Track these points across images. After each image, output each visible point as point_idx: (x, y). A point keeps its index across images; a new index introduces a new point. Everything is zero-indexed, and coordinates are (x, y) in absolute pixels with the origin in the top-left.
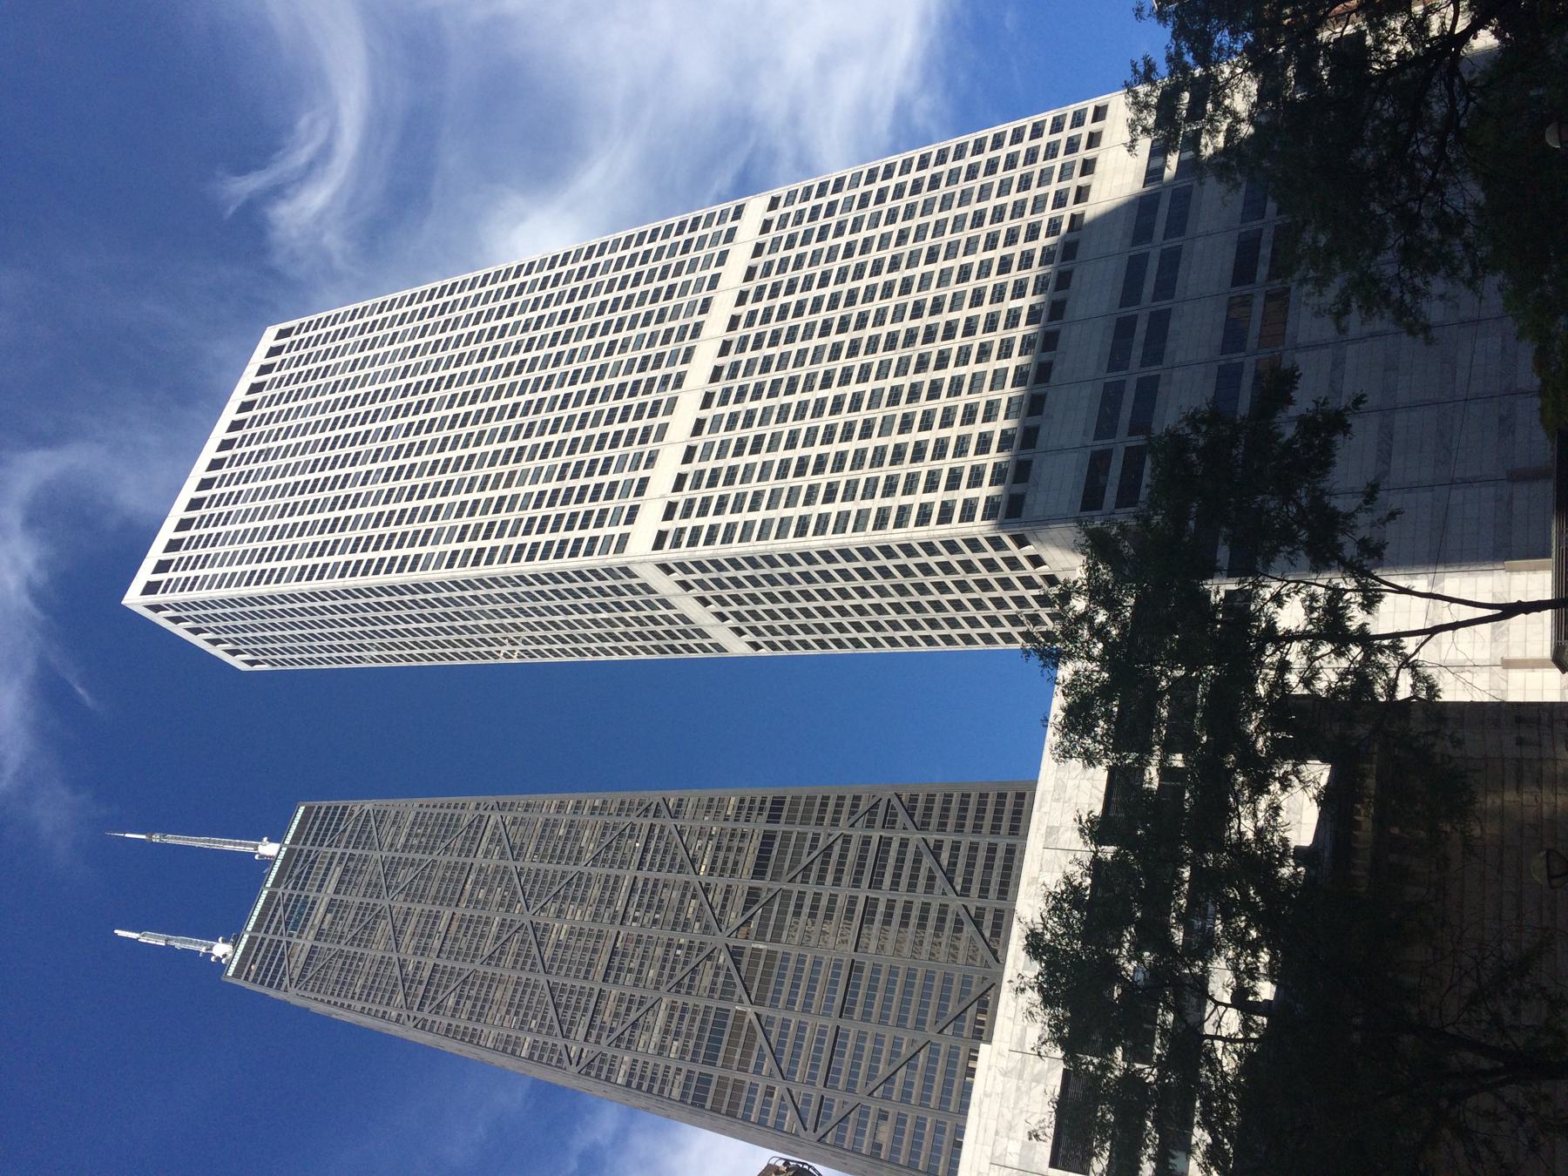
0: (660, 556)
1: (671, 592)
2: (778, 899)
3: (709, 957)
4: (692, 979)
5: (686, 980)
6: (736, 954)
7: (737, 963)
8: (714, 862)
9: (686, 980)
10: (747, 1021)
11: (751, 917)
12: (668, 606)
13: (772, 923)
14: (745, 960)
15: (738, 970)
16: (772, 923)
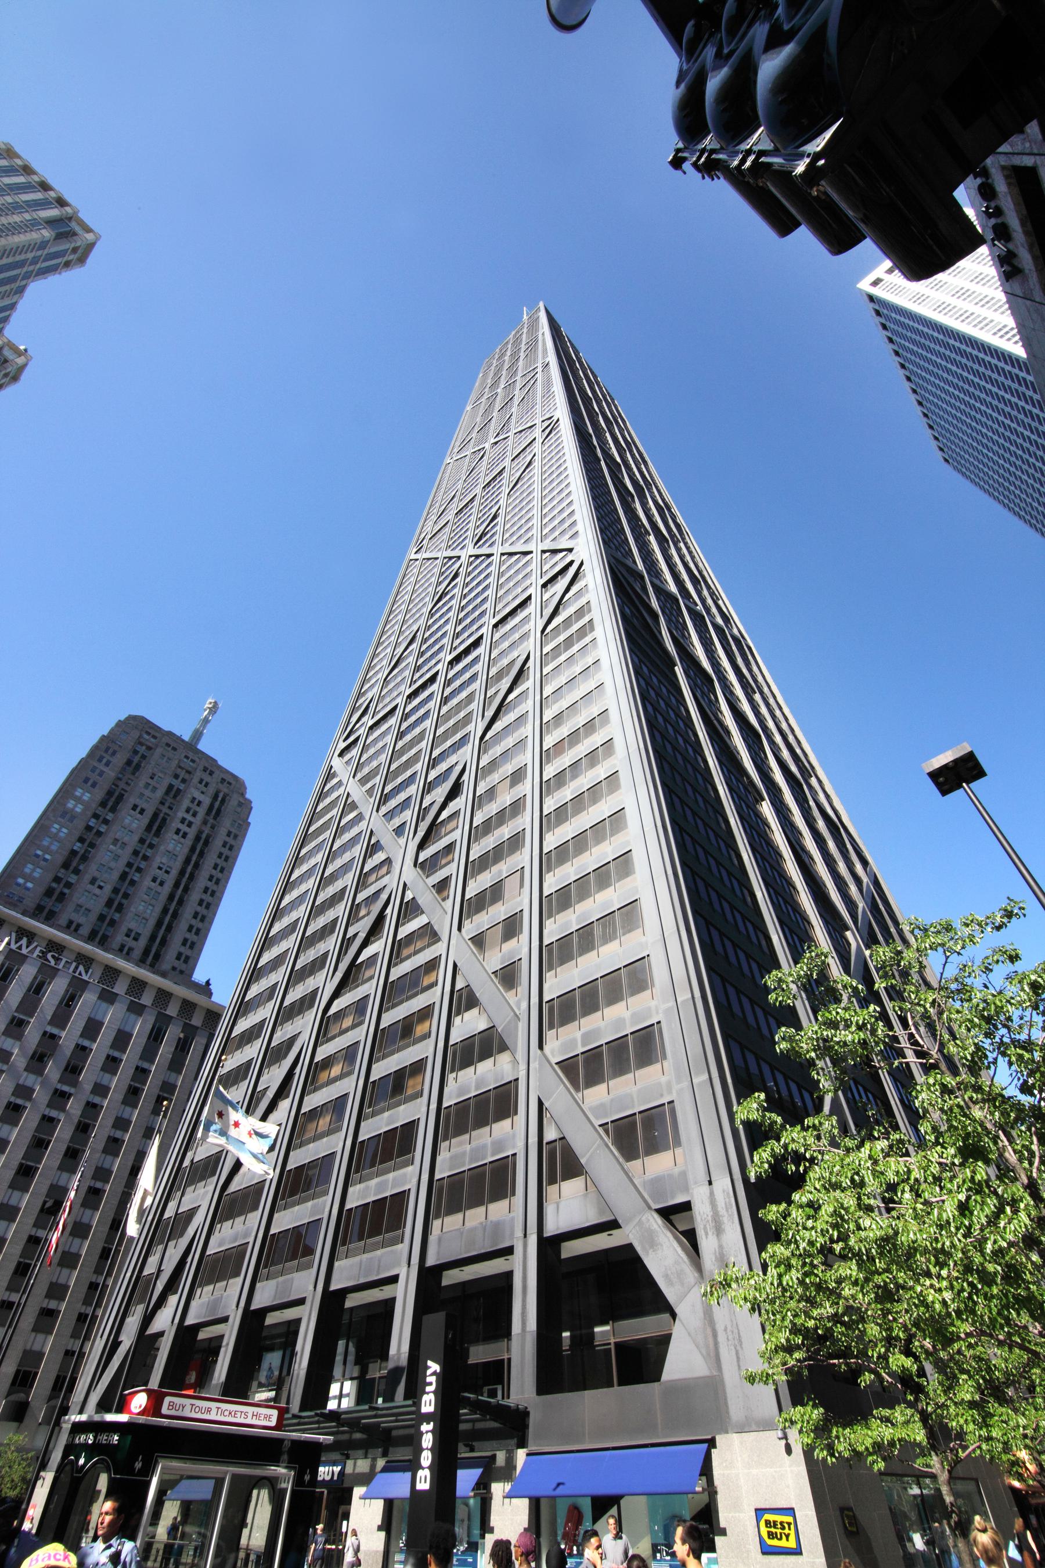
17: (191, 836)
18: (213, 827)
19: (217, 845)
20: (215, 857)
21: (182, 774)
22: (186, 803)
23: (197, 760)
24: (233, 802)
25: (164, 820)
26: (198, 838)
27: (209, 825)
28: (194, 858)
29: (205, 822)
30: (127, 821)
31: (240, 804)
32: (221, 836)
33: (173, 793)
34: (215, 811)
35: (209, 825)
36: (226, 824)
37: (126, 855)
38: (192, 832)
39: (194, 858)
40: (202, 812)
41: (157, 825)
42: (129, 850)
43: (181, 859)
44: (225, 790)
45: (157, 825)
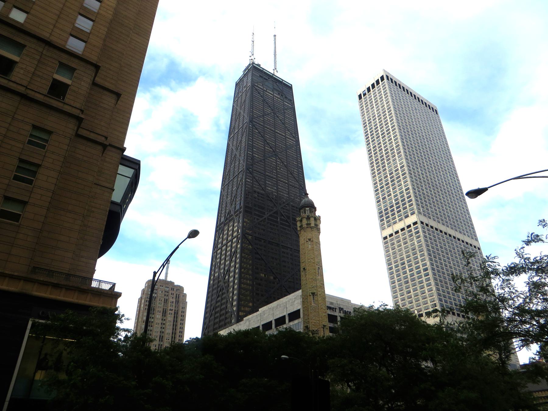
0: (419, 222)
1: (406, 222)
2: (288, 224)
3: (274, 205)
4: (270, 201)
5: (269, 199)
6: (276, 213)
7: (274, 213)
8: (294, 207)
9: (269, 199)
10: (264, 215)
11: (284, 217)
12: (400, 220)
13: (284, 223)
14: (275, 215)
15: (273, 213)
16: (284, 223)
17: (173, 314)
18: (178, 308)
19: (180, 313)
20: (181, 317)
21: (166, 294)
22: (170, 304)
23: (169, 286)
24: (181, 296)
25: (165, 310)
26: (175, 313)
27: (177, 307)
28: (175, 319)
29: (175, 307)
30: (158, 317)
31: (183, 296)
32: (181, 310)
33: (166, 301)
34: (177, 302)
35: (177, 307)
36: (181, 305)
37: (160, 326)
38: (173, 312)
39: (175, 319)
40: (174, 304)
41: (164, 313)
42: (160, 324)
43: (172, 322)
44: (178, 293)
45: (164, 313)
